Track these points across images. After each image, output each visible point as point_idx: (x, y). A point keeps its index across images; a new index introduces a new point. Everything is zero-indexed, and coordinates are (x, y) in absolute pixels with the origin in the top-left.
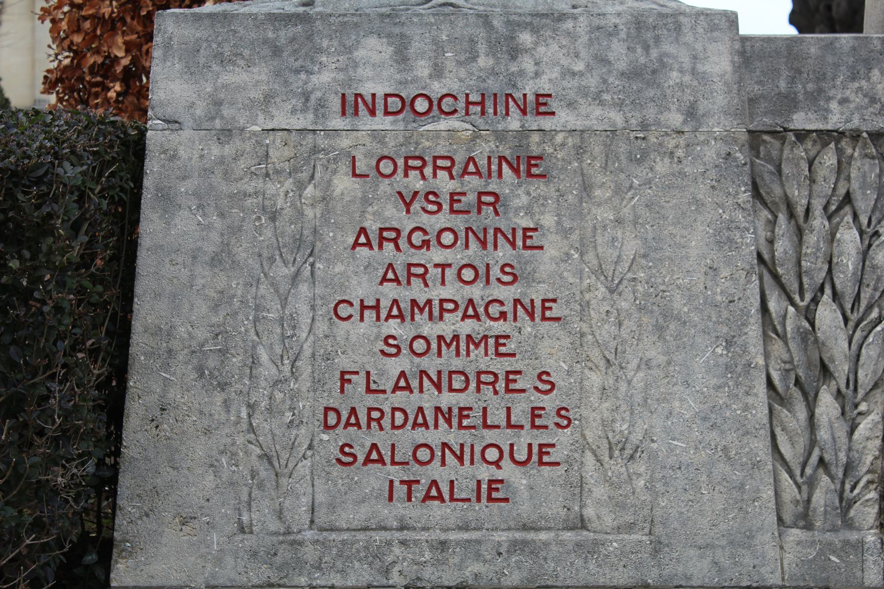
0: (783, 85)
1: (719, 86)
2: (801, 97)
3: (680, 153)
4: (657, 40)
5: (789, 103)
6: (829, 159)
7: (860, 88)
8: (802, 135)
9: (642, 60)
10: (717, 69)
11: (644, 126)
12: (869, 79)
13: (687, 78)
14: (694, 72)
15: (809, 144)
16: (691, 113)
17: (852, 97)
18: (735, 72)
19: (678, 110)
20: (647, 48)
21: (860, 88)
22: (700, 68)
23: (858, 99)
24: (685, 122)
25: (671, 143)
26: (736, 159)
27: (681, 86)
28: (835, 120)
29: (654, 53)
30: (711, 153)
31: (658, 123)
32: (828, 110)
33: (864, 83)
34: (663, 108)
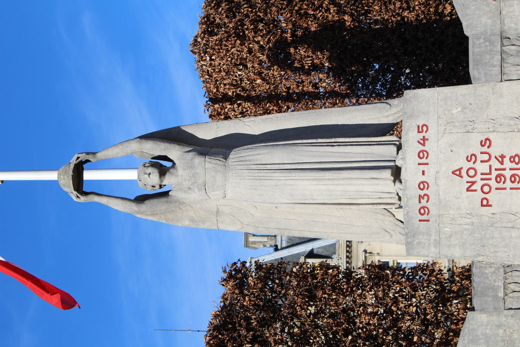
0: (490, 299)
1: (491, 318)
2: (493, 294)
3: (511, 331)
4: (476, 336)
5: (496, 297)
6: (512, 287)
7: (491, 276)
8: (506, 295)
9: (483, 341)
10: (486, 318)
11: (503, 341)
12: (488, 274)
13: (489, 327)
14: (487, 325)
15: (508, 292)
16: (499, 326)
17: (493, 278)
18: (486, 313)
19: (498, 330)
20: (479, 339)
21: (491, 276)
22: (485, 323)
23: (494, 277)
24: (502, 329)
25: (508, 333)
26: (513, 314)
27: (491, 329)
28: (501, 284)
29: (481, 337)
30: (511, 321)
31: (502, 337)
32: (498, 286)
33: (489, 275)
34: (498, 335)
